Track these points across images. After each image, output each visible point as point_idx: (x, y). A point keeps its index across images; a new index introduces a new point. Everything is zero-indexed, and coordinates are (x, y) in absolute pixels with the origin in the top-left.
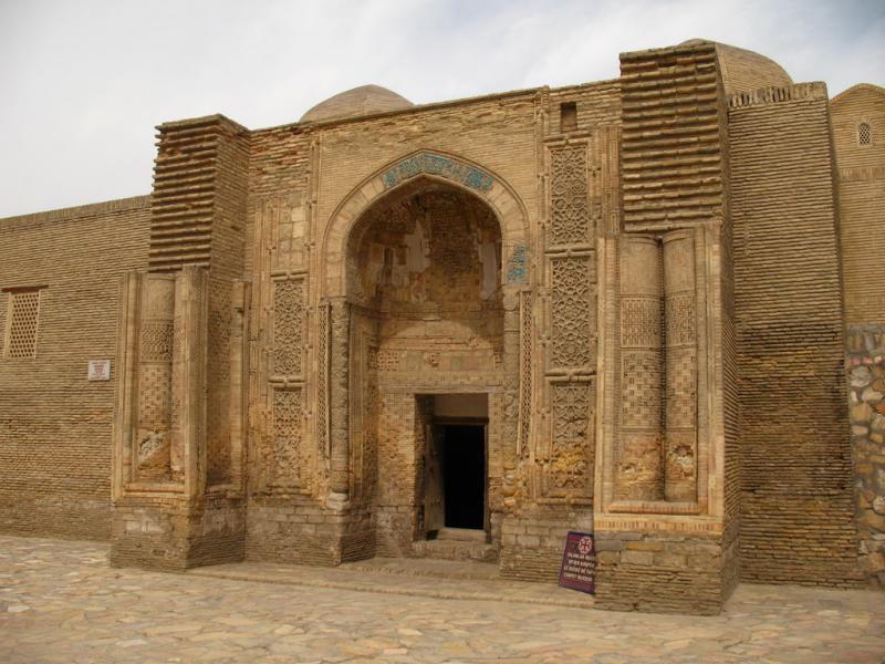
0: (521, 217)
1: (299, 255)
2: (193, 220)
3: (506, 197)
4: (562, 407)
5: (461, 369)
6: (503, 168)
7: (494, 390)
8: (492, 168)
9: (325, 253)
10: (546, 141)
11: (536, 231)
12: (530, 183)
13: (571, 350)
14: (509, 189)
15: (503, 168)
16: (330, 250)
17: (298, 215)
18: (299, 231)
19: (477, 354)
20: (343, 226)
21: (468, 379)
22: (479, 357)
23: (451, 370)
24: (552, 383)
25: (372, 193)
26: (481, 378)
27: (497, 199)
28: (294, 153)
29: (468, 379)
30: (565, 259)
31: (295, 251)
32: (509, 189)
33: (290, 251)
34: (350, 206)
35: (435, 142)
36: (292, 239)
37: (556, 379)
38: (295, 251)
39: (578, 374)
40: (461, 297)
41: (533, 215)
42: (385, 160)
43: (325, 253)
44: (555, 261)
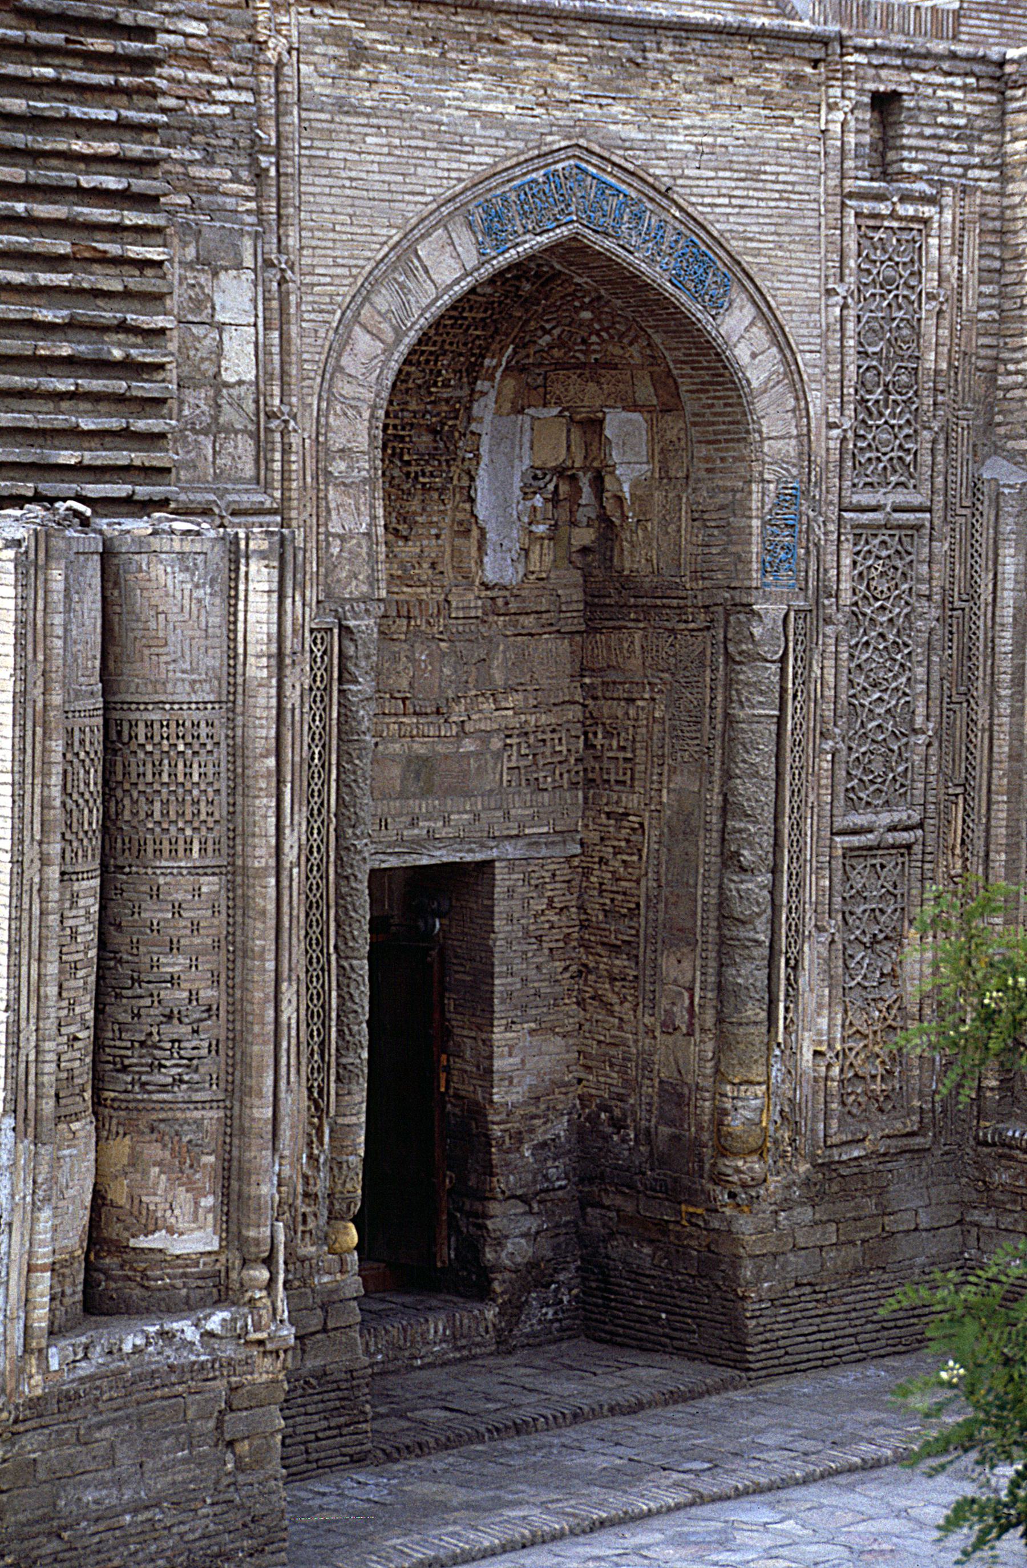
0: (792, 403)
1: (245, 446)
2: (108, 315)
3: (760, 335)
4: (859, 911)
5: (426, 792)
6: (757, 253)
7: (511, 850)
8: (735, 245)
9: (322, 451)
10: (851, 195)
11: (827, 444)
12: (812, 308)
13: (878, 767)
14: (767, 315)
15: (757, 253)
16: (337, 442)
17: (235, 297)
18: (239, 364)
19: (469, 746)
20: (370, 362)
21: (446, 822)
22: (468, 755)
23: (402, 795)
24: (849, 852)
25: (451, 267)
26: (477, 817)
27: (737, 329)
28: (206, 63)
29: (446, 822)
30: (875, 528)
31: (230, 430)
32: (767, 315)
33: (216, 429)
34: (384, 300)
35: (621, 122)
36: (217, 384)
37: (856, 840)
38: (230, 430)
39: (893, 828)
40: (425, 572)
41: (816, 399)
42: (481, 159)
43: (322, 451)
44: (859, 532)
